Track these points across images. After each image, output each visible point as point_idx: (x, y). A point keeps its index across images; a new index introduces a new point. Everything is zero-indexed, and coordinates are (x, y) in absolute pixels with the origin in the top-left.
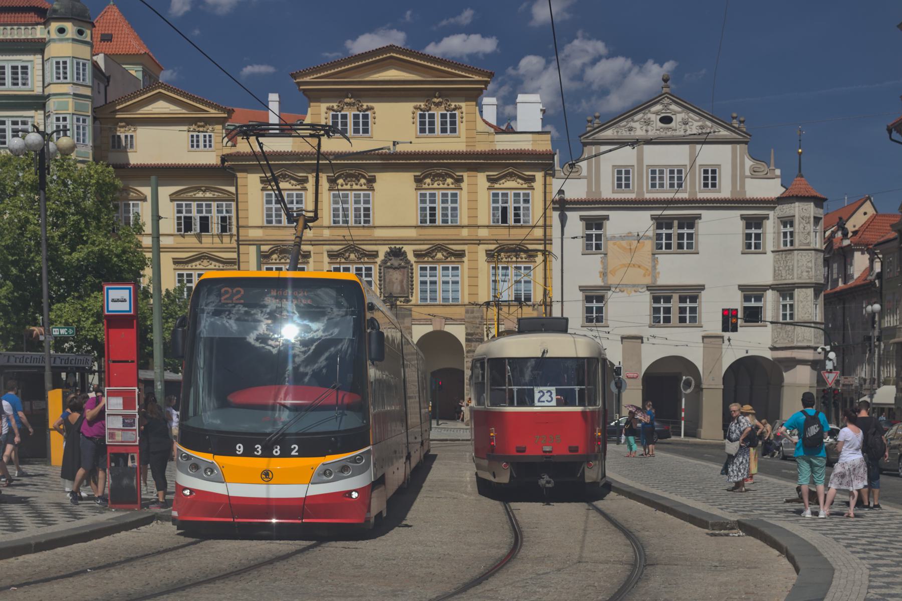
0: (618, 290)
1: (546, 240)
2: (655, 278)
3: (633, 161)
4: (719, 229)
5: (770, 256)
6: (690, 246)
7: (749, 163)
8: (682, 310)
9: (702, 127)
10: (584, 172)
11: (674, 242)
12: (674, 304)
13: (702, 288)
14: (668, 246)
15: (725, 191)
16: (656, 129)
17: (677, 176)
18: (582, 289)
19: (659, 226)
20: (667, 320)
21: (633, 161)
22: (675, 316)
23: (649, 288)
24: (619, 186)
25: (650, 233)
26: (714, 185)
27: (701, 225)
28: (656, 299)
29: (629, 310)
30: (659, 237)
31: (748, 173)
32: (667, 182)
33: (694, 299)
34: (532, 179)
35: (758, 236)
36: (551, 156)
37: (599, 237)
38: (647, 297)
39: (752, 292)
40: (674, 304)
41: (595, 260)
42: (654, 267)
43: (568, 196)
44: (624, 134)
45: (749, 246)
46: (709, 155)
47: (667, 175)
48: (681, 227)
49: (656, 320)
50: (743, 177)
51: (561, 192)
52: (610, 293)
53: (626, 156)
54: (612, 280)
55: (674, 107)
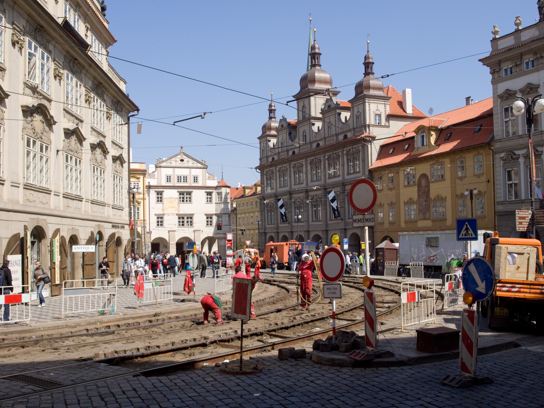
1: (144, 199)
2: (179, 211)
3: (172, 174)
4: (199, 196)
5: (214, 205)
6: (190, 201)
7: (207, 175)
8: (187, 222)
9: (193, 163)
10: (156, 177)
11: (185, 199)
12: (185, 220)
13: (193, 215)
14: (183, 201)
15: (200, 184)
16: (179, 164)
17: (185, 179)
18: (155, 215)
19: (180, 194)
20: (183, 225)
21: (172, 174)
23: (177, 215)
27: (193, 194)
28: (179, 218)
29: (171, 221)
30: (180, 198)
32: (182, 180)
33: (191, 218)
34: (138, 178)
35: (210, 198)
36: (145, 171)
37: (161, 198)
38: (177, 217)
39: (209, 217)
40: (185, 220)
41: (160, 205)
43: (151, 184)
44: (169, 165)
45: (208, 201)
46: (195, 172)
47: (182, 178)
48: (187, 195)
50: (206, 179)
51: (149, 183)
53: (169, 172)
54: (165, 212)
55: (184, 156)
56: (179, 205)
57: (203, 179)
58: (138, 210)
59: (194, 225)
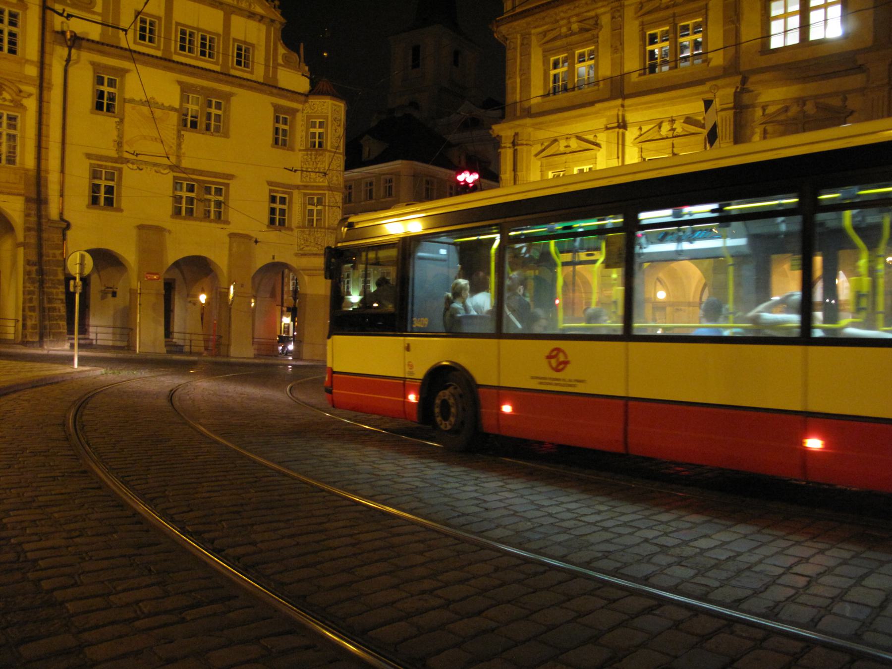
0: (135, 167)
6: (217, 129)
7: (282, 50)
13: (230, 177)
15: (259, 73)
18: (89, 156)
20: (190, 212)
22: (198, 208)
24: (142, 37)
25: (177, 106)
26: (246, 66)
28: (177, 184)
29: (147, 195)
31: (280, 61)
38: (168, 178)
40: (200, 196)
41: (107, 122)
42: (179, 145)
49: (177, 212)
50: (276, 66)
52: (124, 167)
56: (180, 136)
57: (267, 60)
58: (12, 126)
59: (233, 216)
